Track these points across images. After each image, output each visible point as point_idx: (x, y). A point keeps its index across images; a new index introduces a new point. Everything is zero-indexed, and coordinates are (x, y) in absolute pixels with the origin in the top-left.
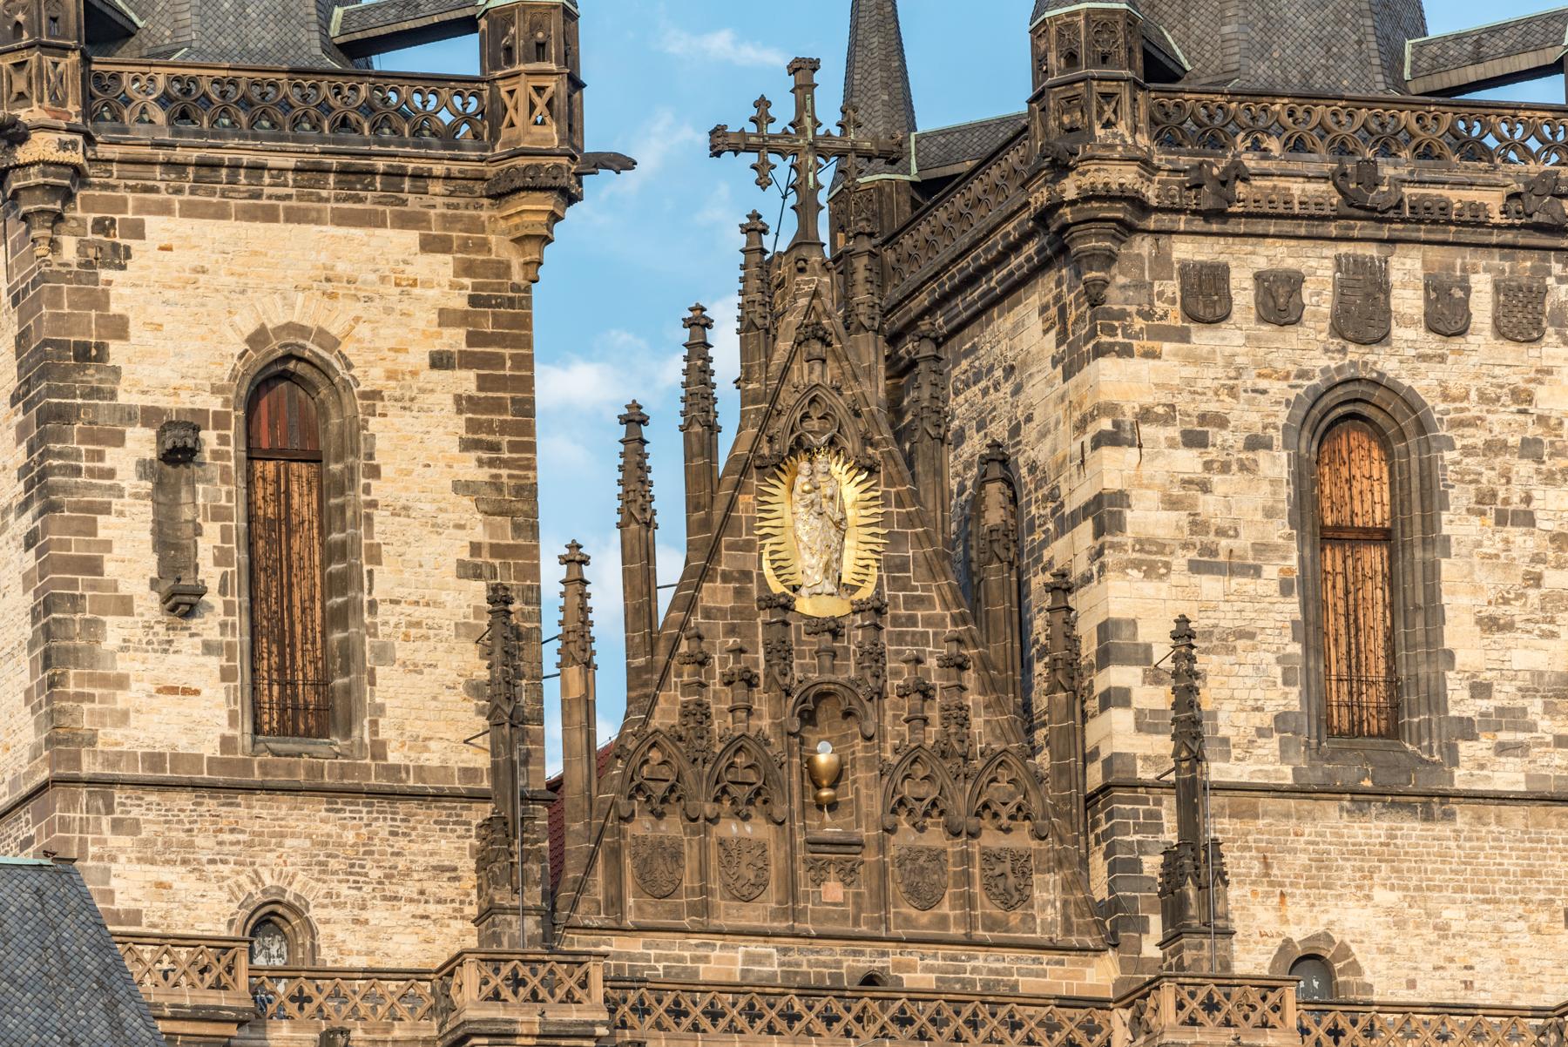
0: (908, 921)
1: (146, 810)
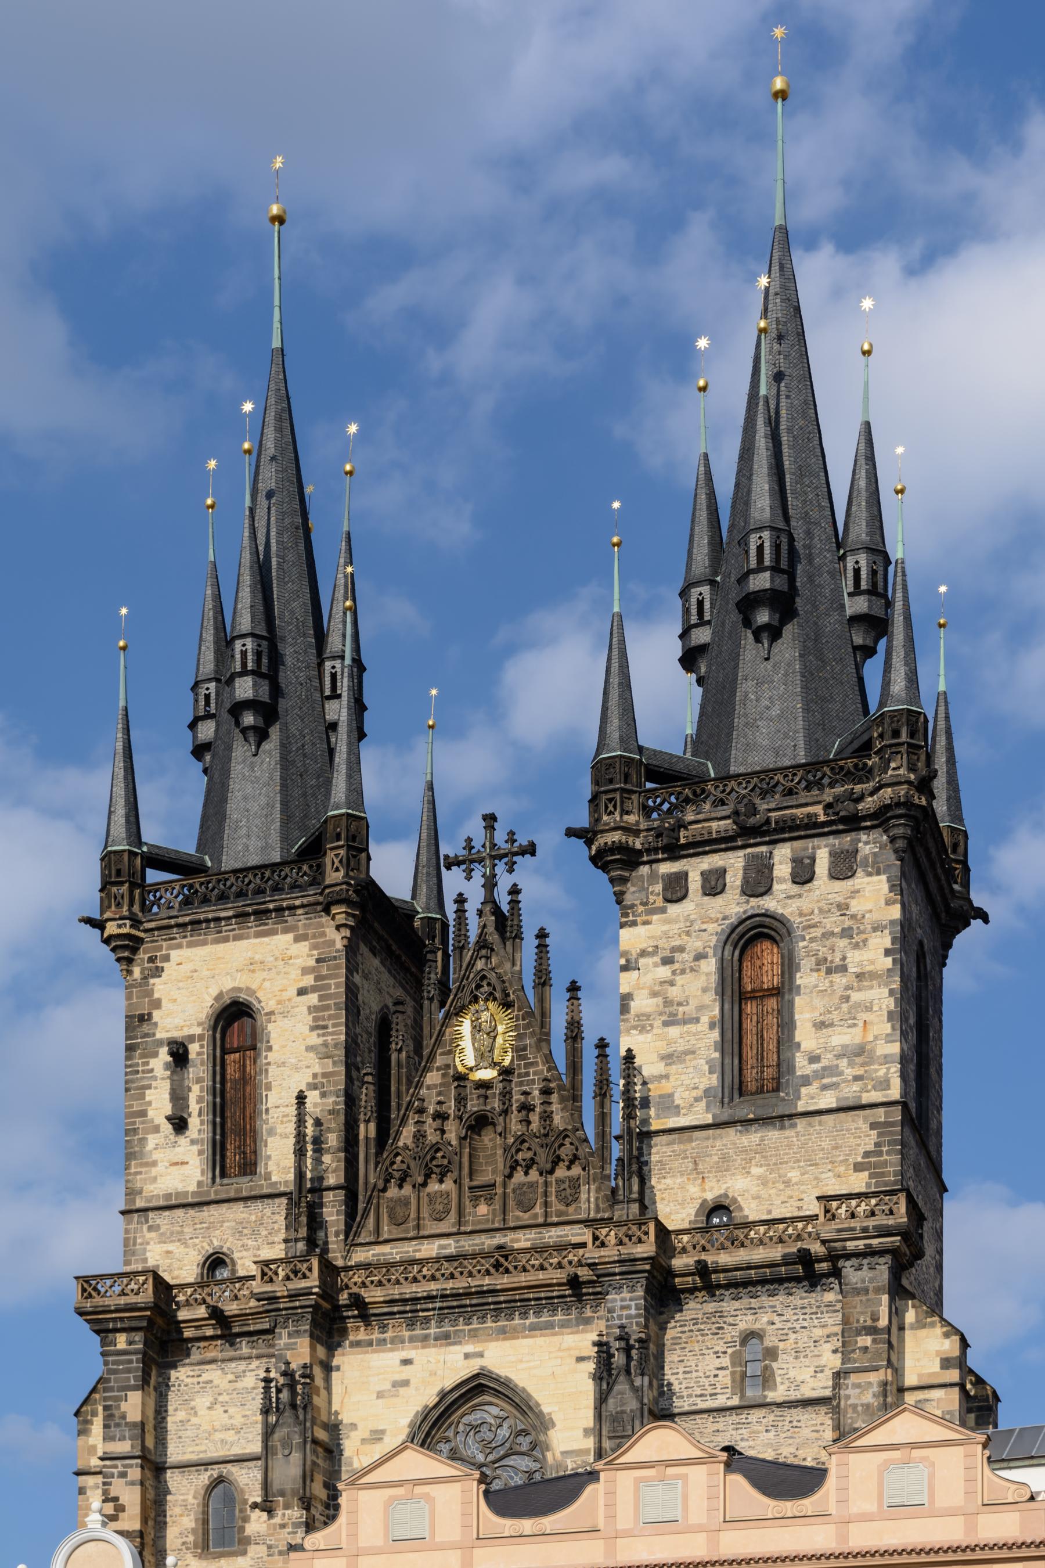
0: (518, 1218)
1: (163, 1219)
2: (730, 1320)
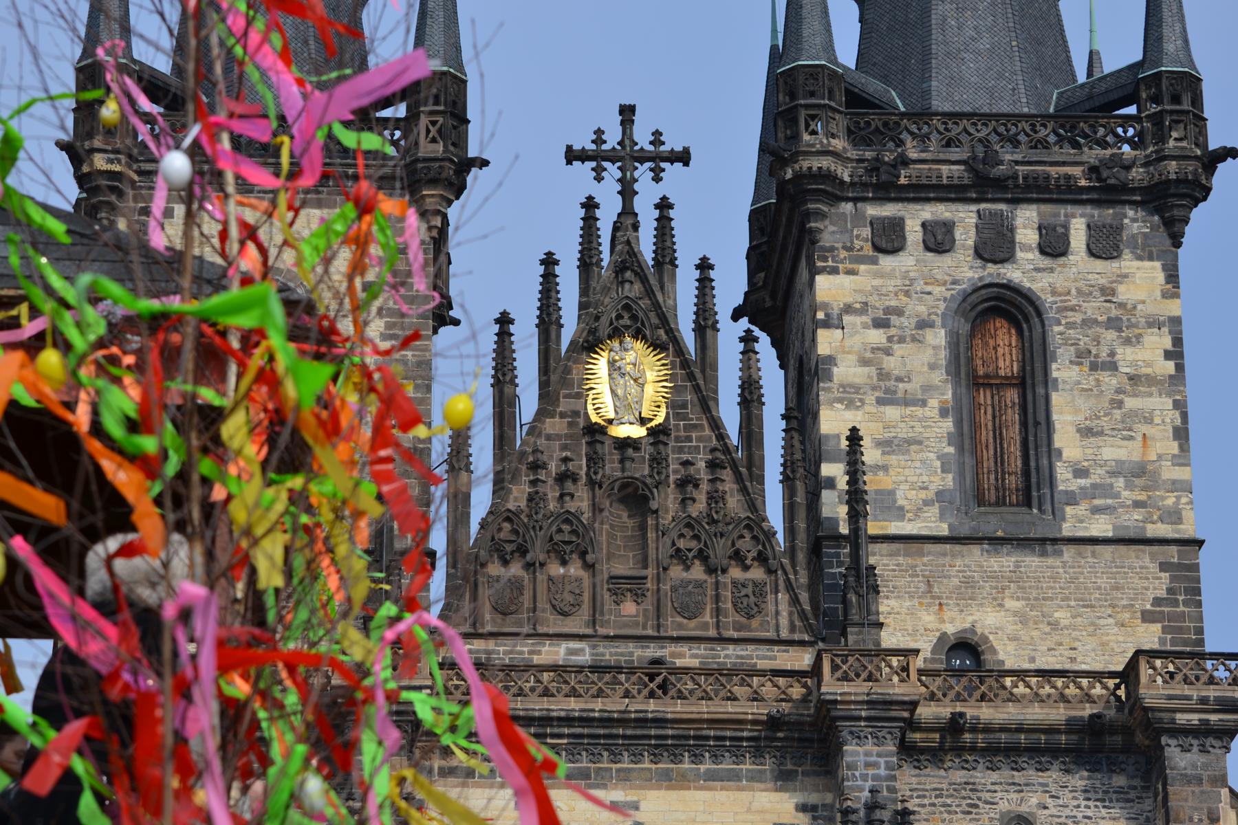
0: (680, 626)
2: (987, 796)
